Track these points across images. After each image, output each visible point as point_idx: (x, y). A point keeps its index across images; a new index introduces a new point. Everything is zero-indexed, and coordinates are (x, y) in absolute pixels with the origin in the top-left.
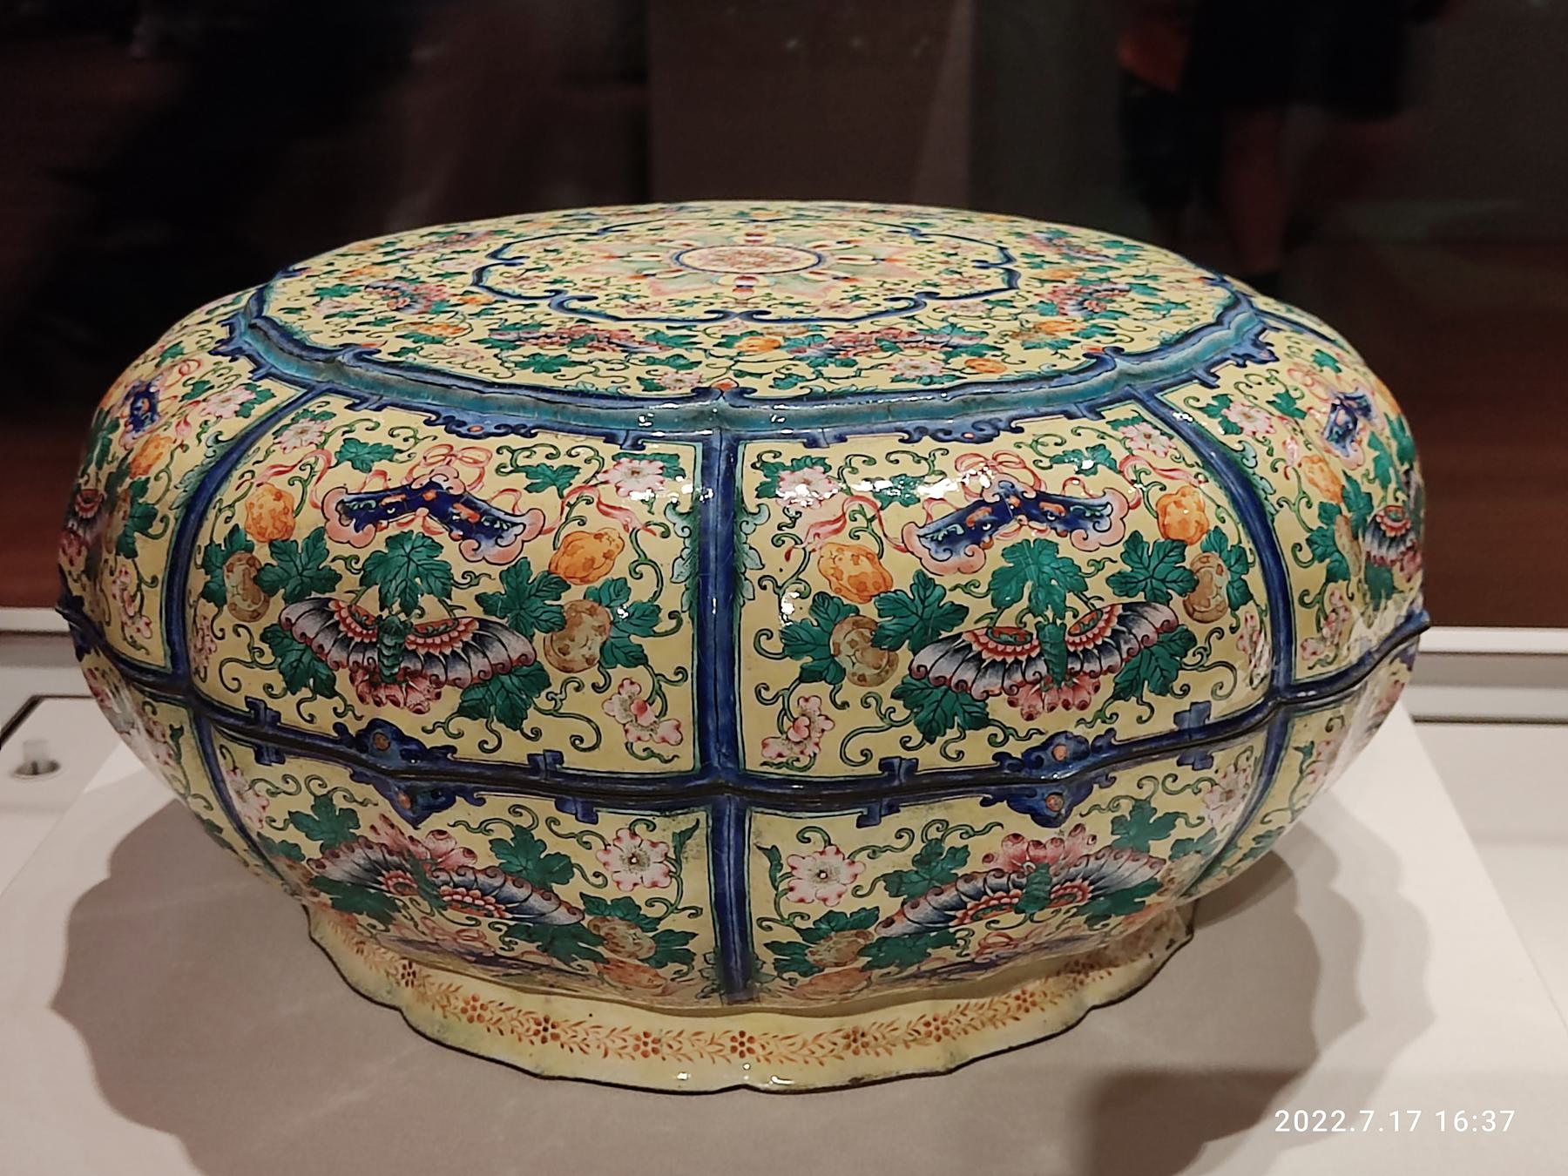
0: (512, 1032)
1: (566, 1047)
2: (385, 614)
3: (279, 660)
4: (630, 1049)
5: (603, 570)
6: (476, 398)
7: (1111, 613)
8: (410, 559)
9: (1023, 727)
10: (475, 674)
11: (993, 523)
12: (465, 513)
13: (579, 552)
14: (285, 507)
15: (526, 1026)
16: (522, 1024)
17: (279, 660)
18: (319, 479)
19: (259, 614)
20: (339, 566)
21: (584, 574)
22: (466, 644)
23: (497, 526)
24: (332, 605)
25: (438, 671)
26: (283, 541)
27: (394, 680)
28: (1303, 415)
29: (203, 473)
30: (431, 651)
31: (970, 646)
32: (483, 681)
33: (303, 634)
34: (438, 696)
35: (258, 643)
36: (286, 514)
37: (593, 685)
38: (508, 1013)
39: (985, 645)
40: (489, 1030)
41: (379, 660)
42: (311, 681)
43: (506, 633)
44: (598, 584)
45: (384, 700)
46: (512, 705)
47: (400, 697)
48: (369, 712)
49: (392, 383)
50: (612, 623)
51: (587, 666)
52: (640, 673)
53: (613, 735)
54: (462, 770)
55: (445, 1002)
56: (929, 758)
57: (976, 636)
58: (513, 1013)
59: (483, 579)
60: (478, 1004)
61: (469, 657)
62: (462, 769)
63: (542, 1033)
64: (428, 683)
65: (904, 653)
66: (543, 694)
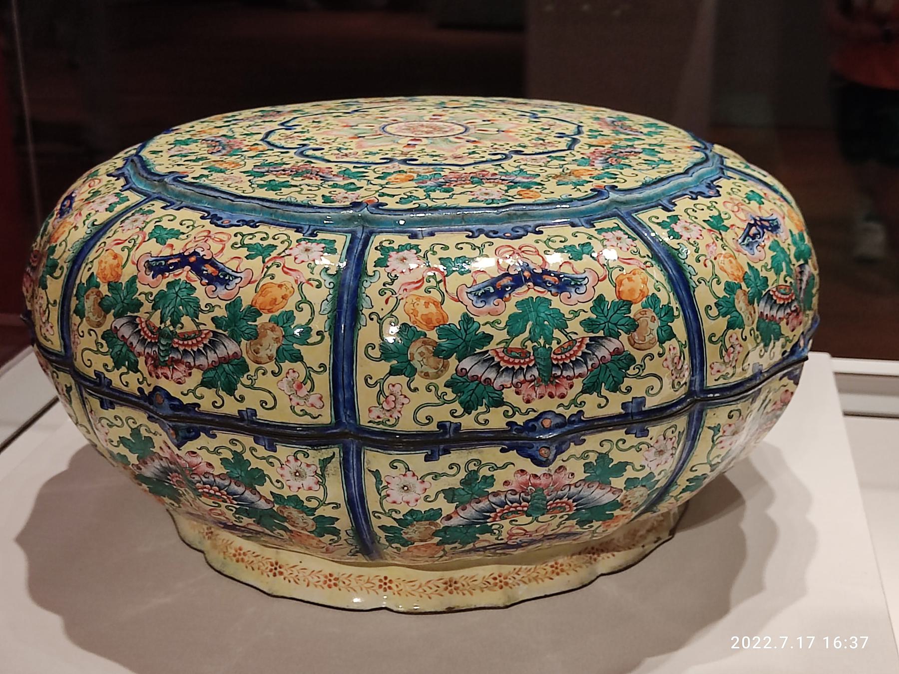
1: (287, 580)
2: (162, 326)
4: (321, 583)
7: (581, 342)
8: (177, 295)
9: (524, 407)
10: (210, 363)
13: (269, 295)
14: (118, 264)
15: (266, 566)
17: (111, 350)
20: (142, 298)
21: (271, 307)
22: (205, 345)
24: (138, 320)
25: (190, 360)
26: (115, 282)
27: (166, 364)
28: (726, 228)
30: (187, 348)
31: (493, 358)
32: (214, 367)
33: (123, 336)
34: (190, 374)
35: (100, 340)
36: (118, 267)
37: (273, 372)
39: (502, 358)
42: (127, 363)
43: (227, 340)
44: (277, 314)
45: (160, 375)
46: (229, 381)
47: (169, 374)
49: (188, 194)
50: (283, 336)
51: (268, 360)
52: (298, 366)
53: (284, 402)
56: (468, 422)
57: (497, 353)
58: (259, 558)
59: (217, 308)
60: (242, 552)
61: (207, 353)
64: (184, 366)
65: (453, 361)
66: (245, 376)
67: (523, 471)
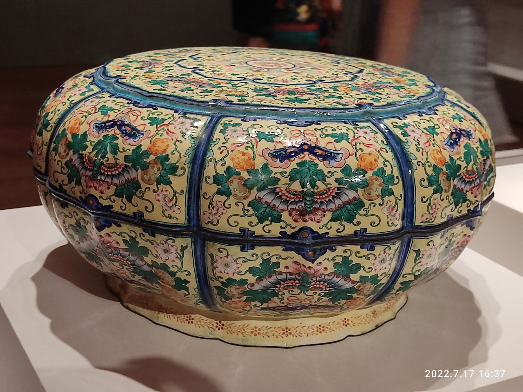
0: (273, 335)
1: (294, 336)
2: (305, 190)
3: (256, 212)
4: (315, 332)
5: (376, 165)
6: (291, 113)
8: (310, 170)
10: (337, 206)
11: (458, 138)
12: (320, 152)
13: (366, 160)
14: (248, 158)
15: (279, 332)
16: (277, 332)
17: (256, 212)
18: (257, 147)
19: (247, 197)
20: (278, 176)
21: (370, 167)
22: (333, 196)
23: (333, 155)
24: (278, 190)
25: (324, 207)
26: (253, 170)
27: (311, 212)
29: (194, 150)
30: (322, 200)
31: (463, 177)
32: (340, 208)
33: (266, 202)
34: (324, 215)
35: (247, 207)
36: (250, 160)
37: (379, 204)
38: (270, 329)
40: (264, 337)
41: (305, 206)
42: (270, 218)
43: (347, 191)
44: (376, 170)
45: (308, 219)
46: (350, 215)
47: (313, 218)
48: (300, 224)
49: (253, 111)
50: (383, 182)
51: (377, 197)
53: (384, 220)
54: (431, 230)
55: (243, 331)
57: (464, 174)
58: (272, 329)
59: (335, 173)
60: (257, 329)
61: (334, 201)
62: (332, 240)
63: (286, 333)
64: (321, 211)
66: (362, 209)
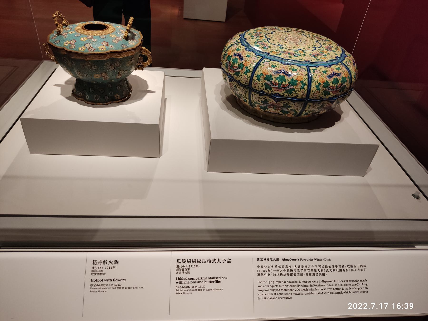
7: (287, 85)
9: (274, 91)
56: (266, 91)
65: (266, 81)
67: (273, 102)
